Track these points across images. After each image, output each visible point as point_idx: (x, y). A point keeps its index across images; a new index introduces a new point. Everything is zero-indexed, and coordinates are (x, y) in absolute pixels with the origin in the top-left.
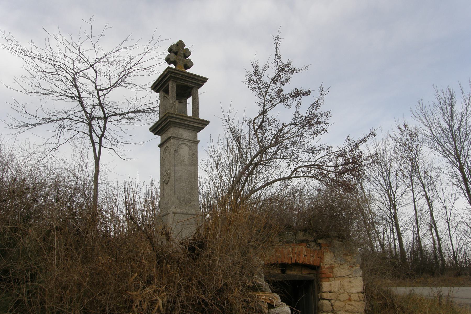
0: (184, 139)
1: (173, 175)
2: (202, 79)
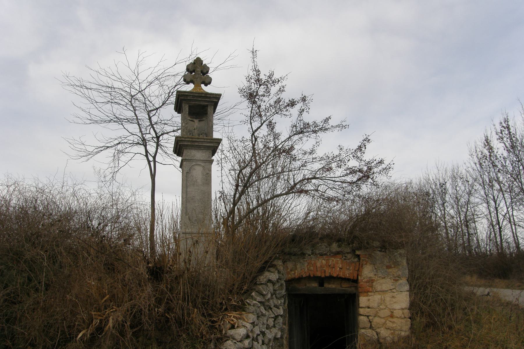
0: (196, 160)
1: (185, 196)
2: (214, 96)
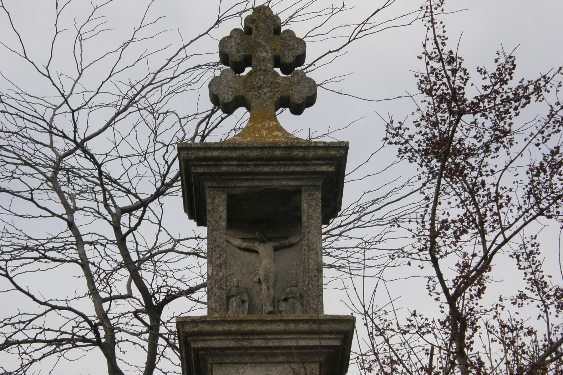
2: (321, 152)
